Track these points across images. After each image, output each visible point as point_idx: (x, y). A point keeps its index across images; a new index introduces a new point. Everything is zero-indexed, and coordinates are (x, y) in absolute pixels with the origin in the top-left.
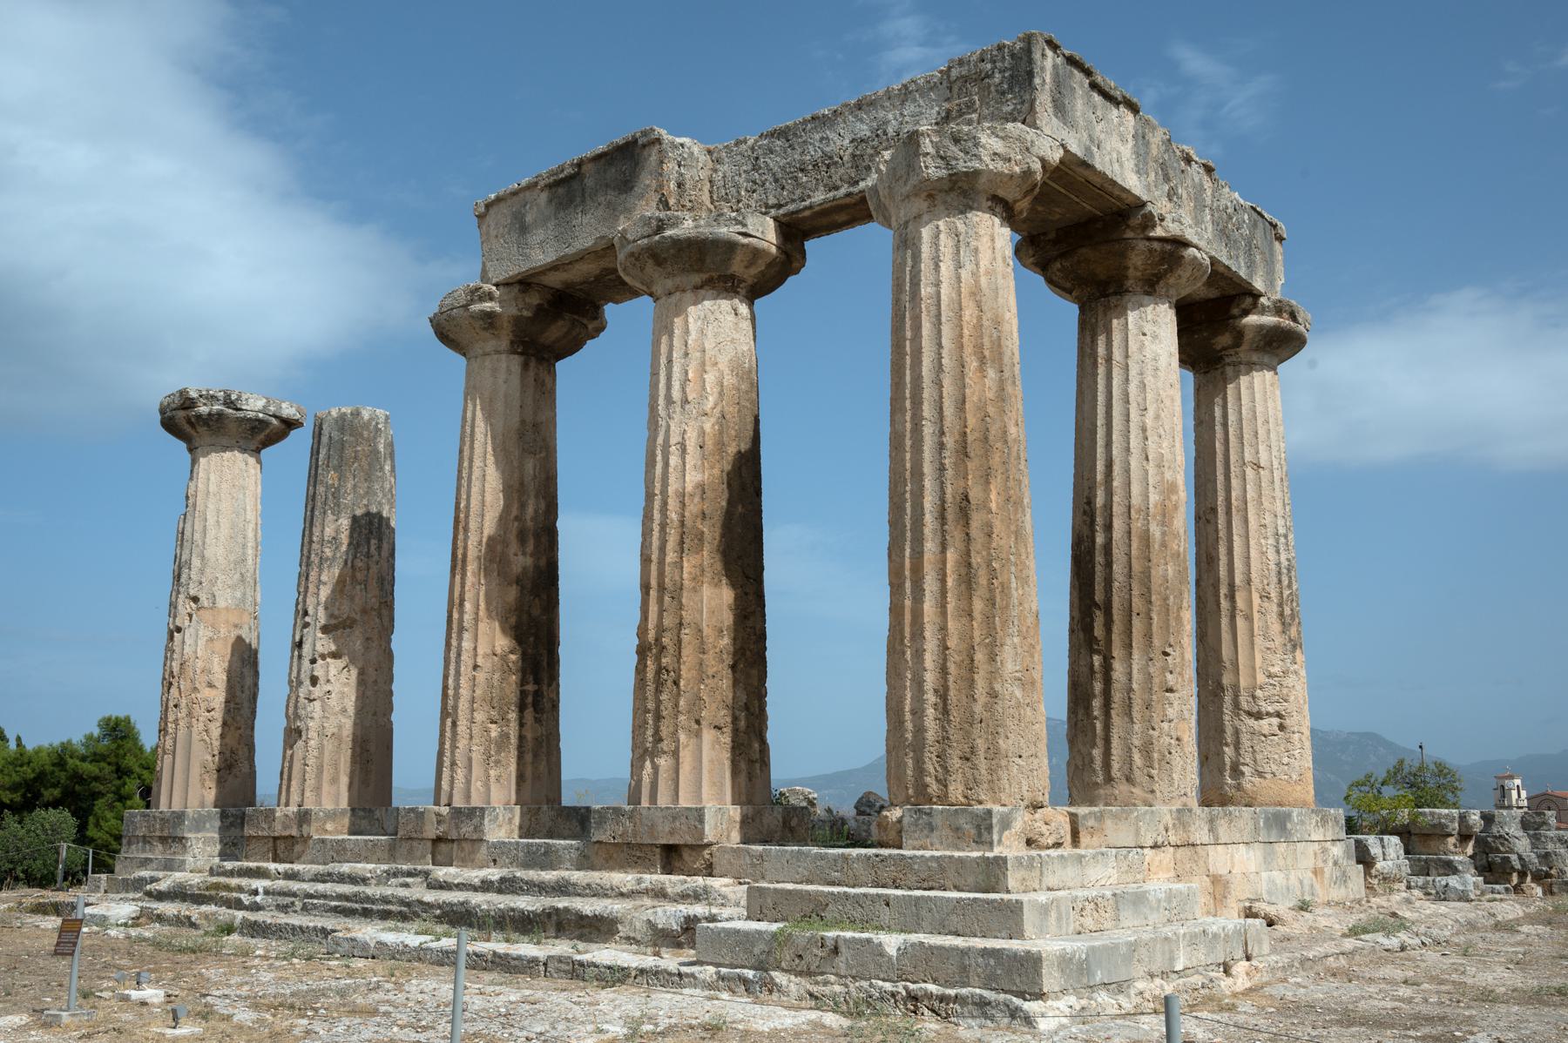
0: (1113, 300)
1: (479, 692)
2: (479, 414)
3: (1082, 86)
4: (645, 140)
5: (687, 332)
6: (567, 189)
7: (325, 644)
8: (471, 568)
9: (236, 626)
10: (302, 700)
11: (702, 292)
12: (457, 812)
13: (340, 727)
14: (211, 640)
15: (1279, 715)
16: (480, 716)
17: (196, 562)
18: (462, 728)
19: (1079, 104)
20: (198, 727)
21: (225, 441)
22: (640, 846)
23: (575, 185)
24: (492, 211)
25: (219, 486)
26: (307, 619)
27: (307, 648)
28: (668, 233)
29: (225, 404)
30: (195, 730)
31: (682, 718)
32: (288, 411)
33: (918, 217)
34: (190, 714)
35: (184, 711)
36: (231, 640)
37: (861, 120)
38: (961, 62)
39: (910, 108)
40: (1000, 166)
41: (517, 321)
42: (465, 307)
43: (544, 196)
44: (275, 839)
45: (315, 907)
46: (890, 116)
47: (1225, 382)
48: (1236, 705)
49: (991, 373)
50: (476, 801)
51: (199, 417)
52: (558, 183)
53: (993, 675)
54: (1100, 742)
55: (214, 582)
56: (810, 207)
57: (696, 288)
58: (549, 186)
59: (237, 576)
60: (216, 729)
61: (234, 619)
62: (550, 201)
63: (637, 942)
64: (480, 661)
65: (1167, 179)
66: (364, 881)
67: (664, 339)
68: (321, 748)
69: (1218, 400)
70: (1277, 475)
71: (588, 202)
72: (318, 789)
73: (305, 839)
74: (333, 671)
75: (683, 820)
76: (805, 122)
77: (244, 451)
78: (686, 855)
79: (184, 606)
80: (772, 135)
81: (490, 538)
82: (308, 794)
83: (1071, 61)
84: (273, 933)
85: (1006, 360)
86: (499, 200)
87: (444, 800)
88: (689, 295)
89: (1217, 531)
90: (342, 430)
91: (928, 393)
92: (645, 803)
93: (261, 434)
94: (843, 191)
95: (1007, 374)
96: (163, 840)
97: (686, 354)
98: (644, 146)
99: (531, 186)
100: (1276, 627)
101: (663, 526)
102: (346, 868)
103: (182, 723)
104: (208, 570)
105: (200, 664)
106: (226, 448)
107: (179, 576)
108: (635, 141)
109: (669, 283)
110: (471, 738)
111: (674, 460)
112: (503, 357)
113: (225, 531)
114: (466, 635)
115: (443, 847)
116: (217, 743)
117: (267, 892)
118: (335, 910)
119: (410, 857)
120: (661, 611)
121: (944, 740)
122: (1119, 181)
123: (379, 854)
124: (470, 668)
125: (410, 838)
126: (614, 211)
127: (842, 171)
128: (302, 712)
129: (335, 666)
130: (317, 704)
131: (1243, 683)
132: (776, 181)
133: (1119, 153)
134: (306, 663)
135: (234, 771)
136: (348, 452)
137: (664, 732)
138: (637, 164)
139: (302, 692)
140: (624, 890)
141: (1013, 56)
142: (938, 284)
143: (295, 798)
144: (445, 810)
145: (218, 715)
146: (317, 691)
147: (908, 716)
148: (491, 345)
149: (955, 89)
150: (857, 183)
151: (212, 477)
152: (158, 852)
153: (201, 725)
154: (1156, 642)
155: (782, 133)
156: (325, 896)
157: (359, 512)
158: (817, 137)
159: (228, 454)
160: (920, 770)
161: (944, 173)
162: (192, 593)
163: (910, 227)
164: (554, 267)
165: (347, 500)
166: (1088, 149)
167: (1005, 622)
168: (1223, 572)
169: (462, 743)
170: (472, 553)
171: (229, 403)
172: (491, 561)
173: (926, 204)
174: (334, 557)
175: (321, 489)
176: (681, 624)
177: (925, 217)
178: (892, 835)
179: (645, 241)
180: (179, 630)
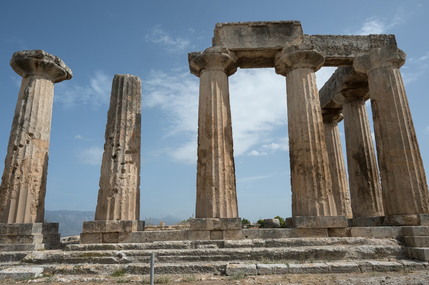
0: (361, 101)
1: (226, 179)
2: (217, 88)
4: (297, 24)
5: (311, 79)
6: (261, 29)
7: (128, 158)
8: (219, 137)
9: (46, 148)
10: (118, 178)
11: (312, 70)
12: (226, 221)
13: (133, 189)
14: (38, 152)
16: (227, 187)
17: (33, 120)
18: (221, 190)
20: (30, 188)
21: (47, 76)
22: (319, 229)
23: (265, 29)
24: (224, 27)
25: (44, 92)
26: (120, 147)
27: (120, 159)
28: (314, 50)
29: (55, 61)
30: (29, 189)
31: (327, 189)
32: (71, 73)
33: (390, 66)
34: (27, 182)
35: (24, 181)
36: (45, 154)
37: (345, 41)
38: (374, 35)
39: (359, 42)
41: (233, 62)
42: (220, 53)
43: (250, 29)
44: (103, 233)
45: (169, 259)
46: (353, 42)
47: (333, 127)
48: (343, 197)
50: (228, 216)
51: (43, 63)
52: (257, 26)
54: (373, 202)
55: (40, 129)
56: (334, 57)
57: (311, 68)
58: (253, 26)
59: (48, 129)
60: (37, 190)
61: (46, 146)
62: (253, 31)
63: (356, 258)
64: (226, 168)
66: (184, 247)
67: (304, 79)
68: (127, 198)
69: (332, 130)
71: (271, 34)
72: (126, 213)
73: (126, 233)
74: (131, 169)
75: (338, 220)
76: (327, 36)
77: (52, 82)
78: (337, 231)
79: (24, 137)
80: (317, 36)
81: (225, 128)
82: (122, 215)
84: (160, 271)
86: (229, 25)
87: (214, 216)
88: (310, 70)
89: (335, 158)
90: (132, 82)
91: (403, 109)
92: (318, 215)
93: (60, 76)
94: (344, 56)
96: (10, 237)
97: (312, 85)
98: (295, 25)
99: (247, 24)
101: (313, 133)
102: (168, 243)
103: (22, 186)
104: (38, 124)
105: (33, 162)
106: (47, 79)
107: (22, 124)
108: (292, 23)
109: (304, 65)
110: (225, 194)
111: (313, 114)
112: (223, 72)
113: (45, 111)
114: (219, 159)
115: (215, 233)
116: (37, 195)
117: (128, 255)
118: (184, 259)
119: (197, 236)
120: (316, 157)
121: (424, 197)
123: (178, 237)
124: (222, 170)
125: (198, 230)
126: (283, 40)
127: (342, 51)
128: (118, 183)
129: (132, 166)
130: (125, 180)
131: (344, 192)
132: (320, 48)
134: (119, 165)
135: (41, 207)
136: (134, 90)
137: (323, 193)
138: (292, 29)
139: (118, 175)
140: (329, 243)
141: (389, 38)
142: (399, 84)
143: (116, 216)
144: (218, 220)
145: (39, 183)
146: (125, 175)
147: (413, 190)
148: (220, 68)
149: (373, 41)
150: (348, 55)
151: (42, 88)
152: (8, 242)
153: (32, 187)
155: (320, 37)
156: (173, 254)
157: (137, 112)
158: (332, 41)
159: (48, 81)
160: (420, 205)
161: (399, 58)
162: (30, 131)
163: (388, 68)
164: (251, 50)
165: (134, 107)
168: (337, 167)
169: (221, 196)
170: (219, 132)
171: (57, 62)
172: (225, 135)
173: (392, 64)
174: (131, 127)
175: (124, 101)
176: (323, 161)
177: (392, 67)
178: (416, 222)
179: (307, 50)
180: (21, 146)
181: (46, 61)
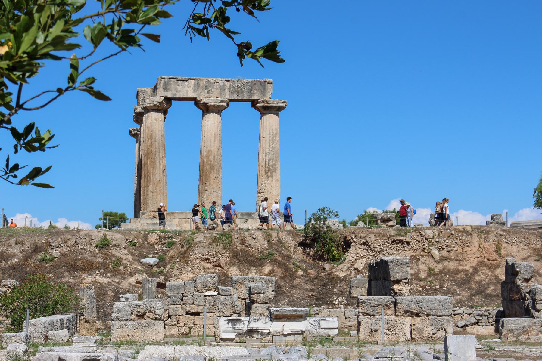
3: (174, 82)
15: (263, 192)
19: (172, 86)
40: (149, 105)
49: (150, 141)
53: (147, 191)
65: (206, 88)
70: (268, 139)
83: (170, 79)
85: (154, 138)
95: (153, 140)
100: (264, 173)
122: (186, 97)
133: (187, 91)
154: (204, 181)
166: (175, 94)
167: (150, 183)
181: (133, 133)
